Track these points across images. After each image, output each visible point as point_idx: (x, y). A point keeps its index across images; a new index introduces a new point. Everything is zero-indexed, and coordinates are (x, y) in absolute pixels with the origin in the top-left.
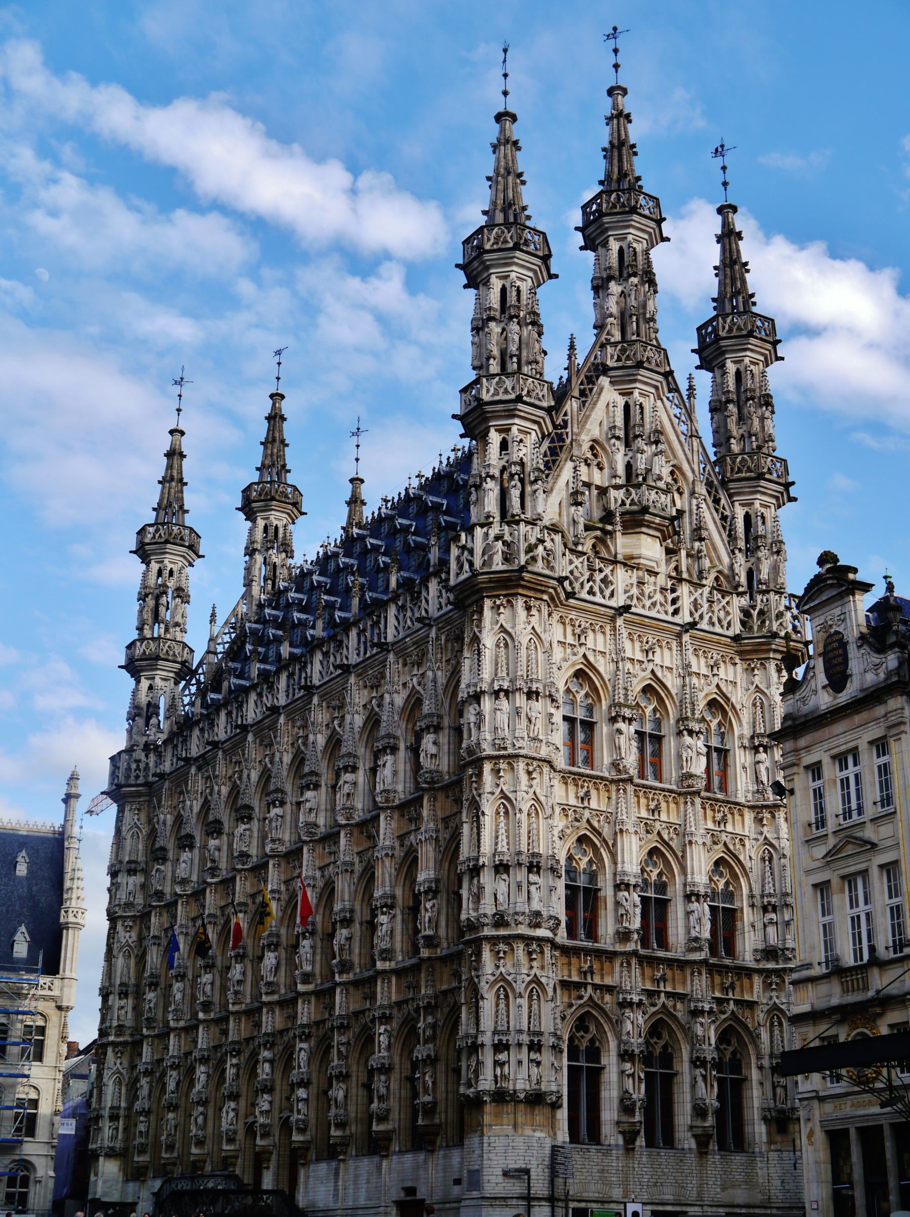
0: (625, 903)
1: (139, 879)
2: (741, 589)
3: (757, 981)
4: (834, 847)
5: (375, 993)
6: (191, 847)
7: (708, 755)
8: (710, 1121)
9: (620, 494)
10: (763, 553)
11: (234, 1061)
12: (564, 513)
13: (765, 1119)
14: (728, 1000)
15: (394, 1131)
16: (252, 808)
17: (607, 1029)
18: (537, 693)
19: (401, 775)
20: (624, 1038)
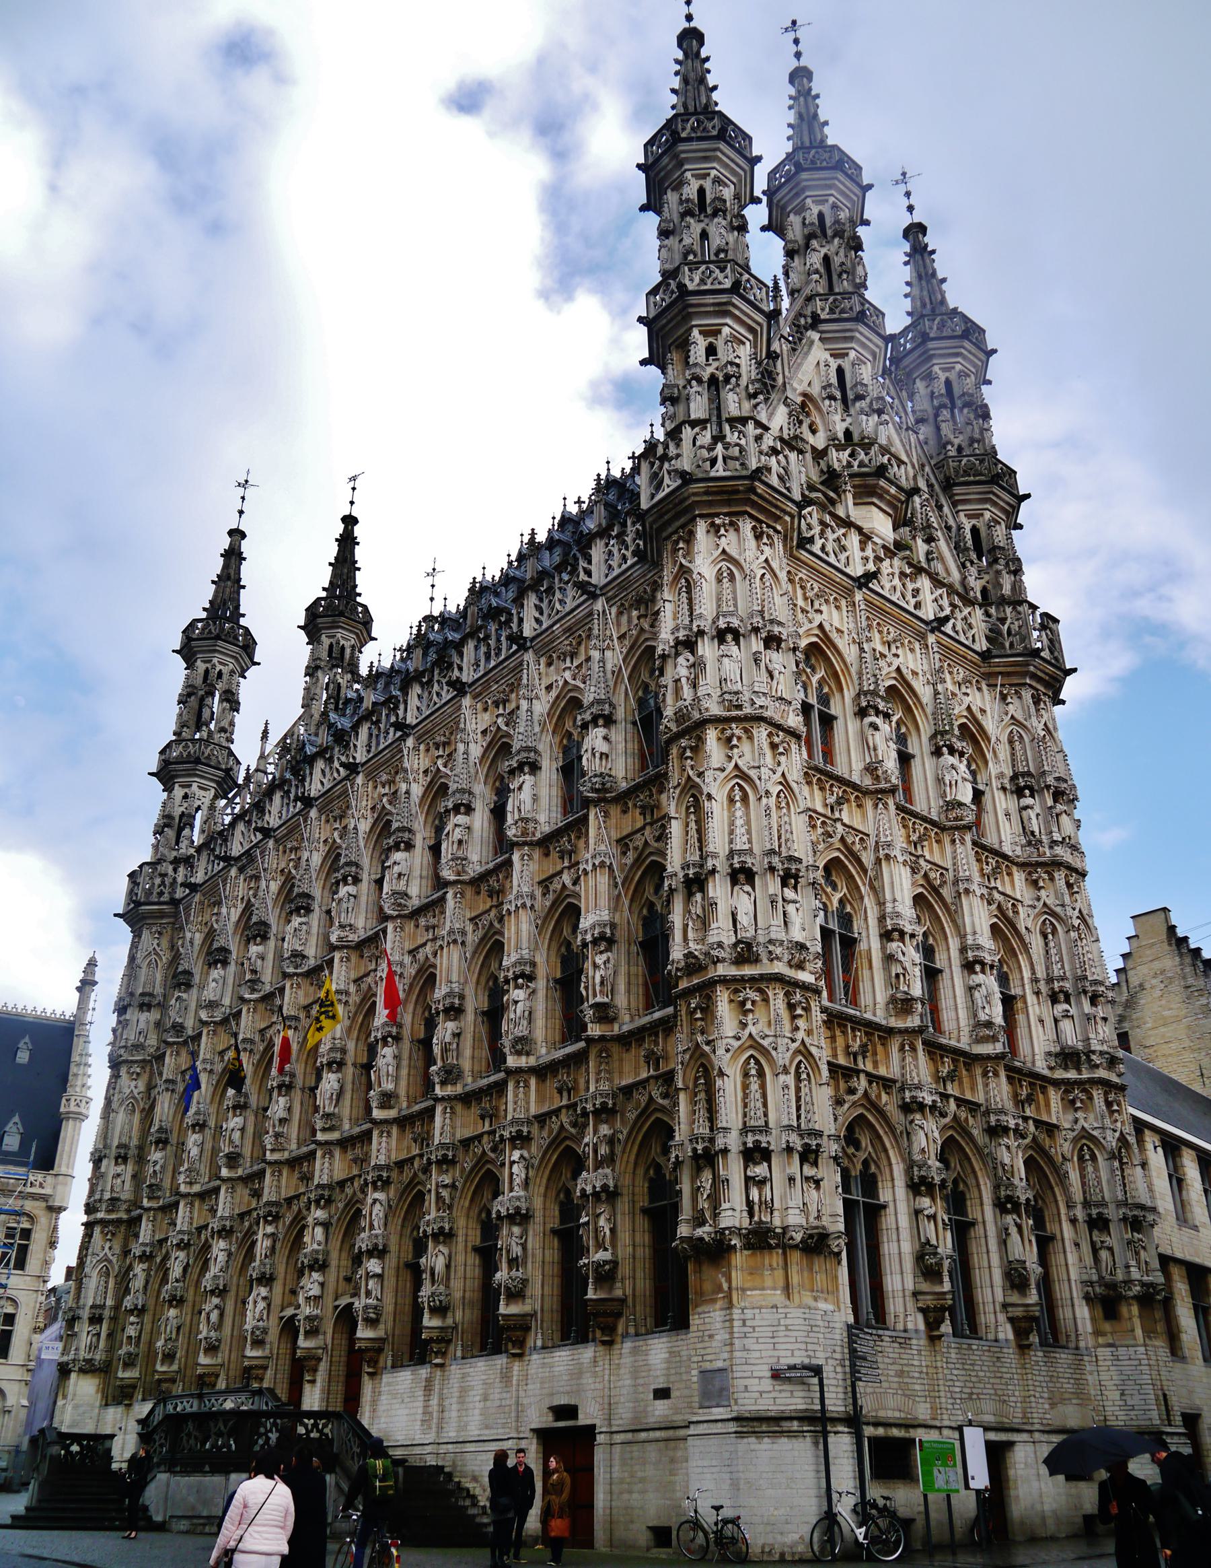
0: (901, 958)
1: (154, 1015)
3: (1054, 1096)
6: (225, 963)
8: (1033, 1297)
11: (270, 1229)
13: (1087, 1298)
15: (533, 1315)
16: (313, 898)
19: (544, 802)
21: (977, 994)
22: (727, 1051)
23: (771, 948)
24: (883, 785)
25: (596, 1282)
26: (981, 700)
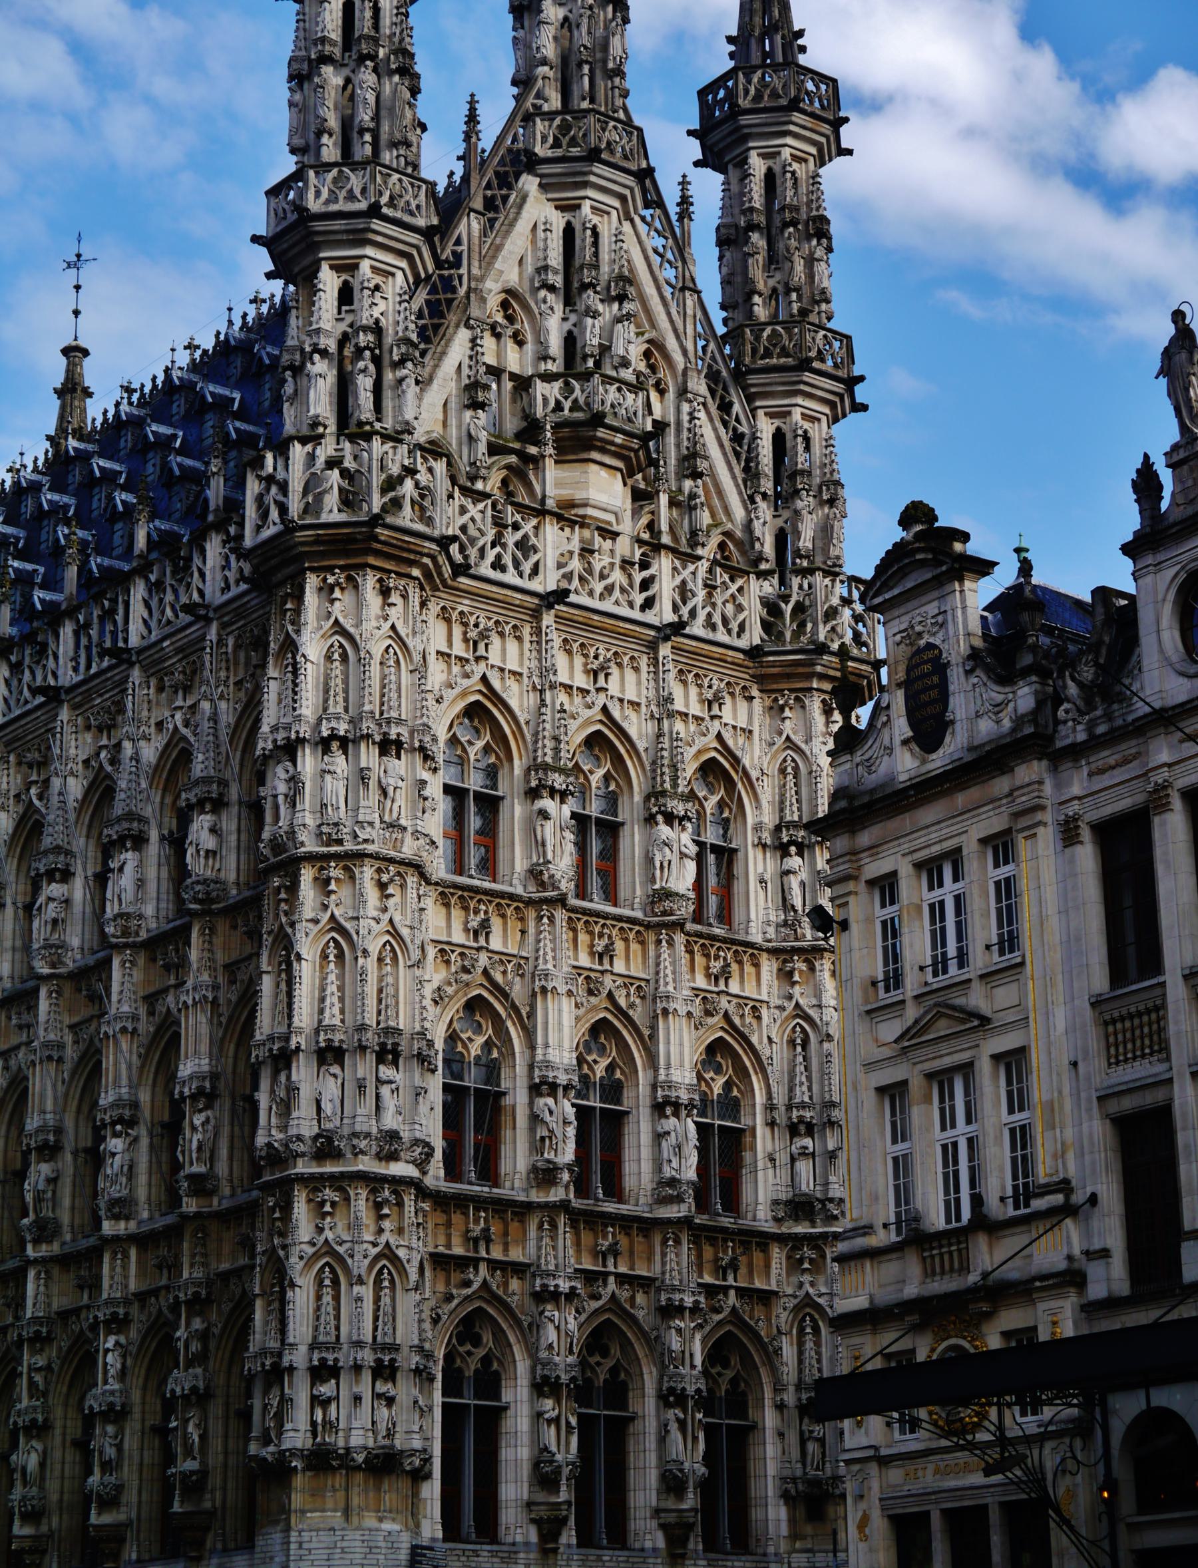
0: (548, 1118)
2: (763, 566)
3: (777, 1255)
4: (916, 1022)
5: (99, 1277)
7: (700, 859)
8: (691, 1500)
9: (553, 390)
10: (804, 503)
12: (453, 422)
13: (786, 1496)
14: (725, 1290)
15: (128, 1524)
17: (512, 1339)
18: (398, 744)
19: (152, 887)
20: (543, 1354)
21: (664, 1143)
22: (301, 1258)
23: (355, 1141)
25: (182, 1495)
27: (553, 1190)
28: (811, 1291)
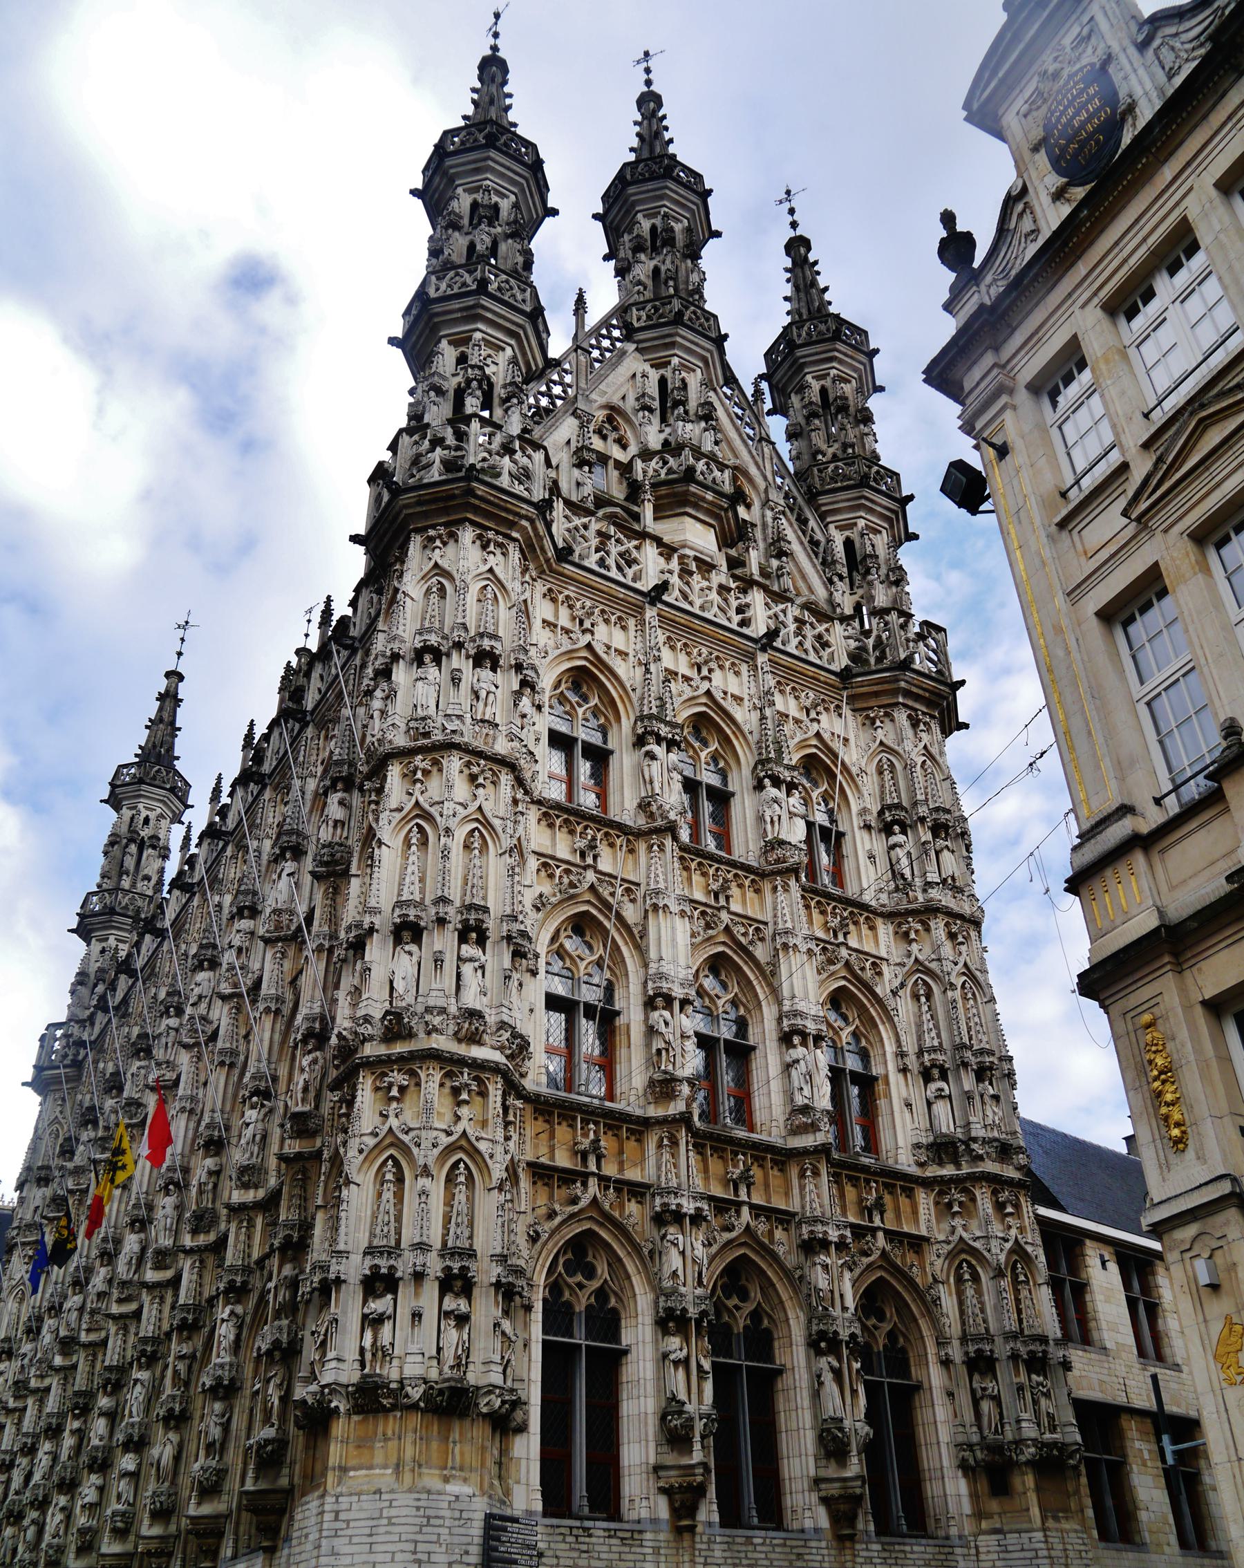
0: (662, 1028)
3: (925, 1200)
8: (855, 1466)
11: (76, 1425)
13: (964, 1466)
14: (874, 1230)
15: (228, 1516)
17: (631, 1268)
20: (667, 1284)
21: (794, 1072)
22: (361, 1151)
23: (428, 1017)
24: (659, 823)
25: (258, 1470)
26: (839, 726)
27: (672, 1104)
28: (965, 1235)
